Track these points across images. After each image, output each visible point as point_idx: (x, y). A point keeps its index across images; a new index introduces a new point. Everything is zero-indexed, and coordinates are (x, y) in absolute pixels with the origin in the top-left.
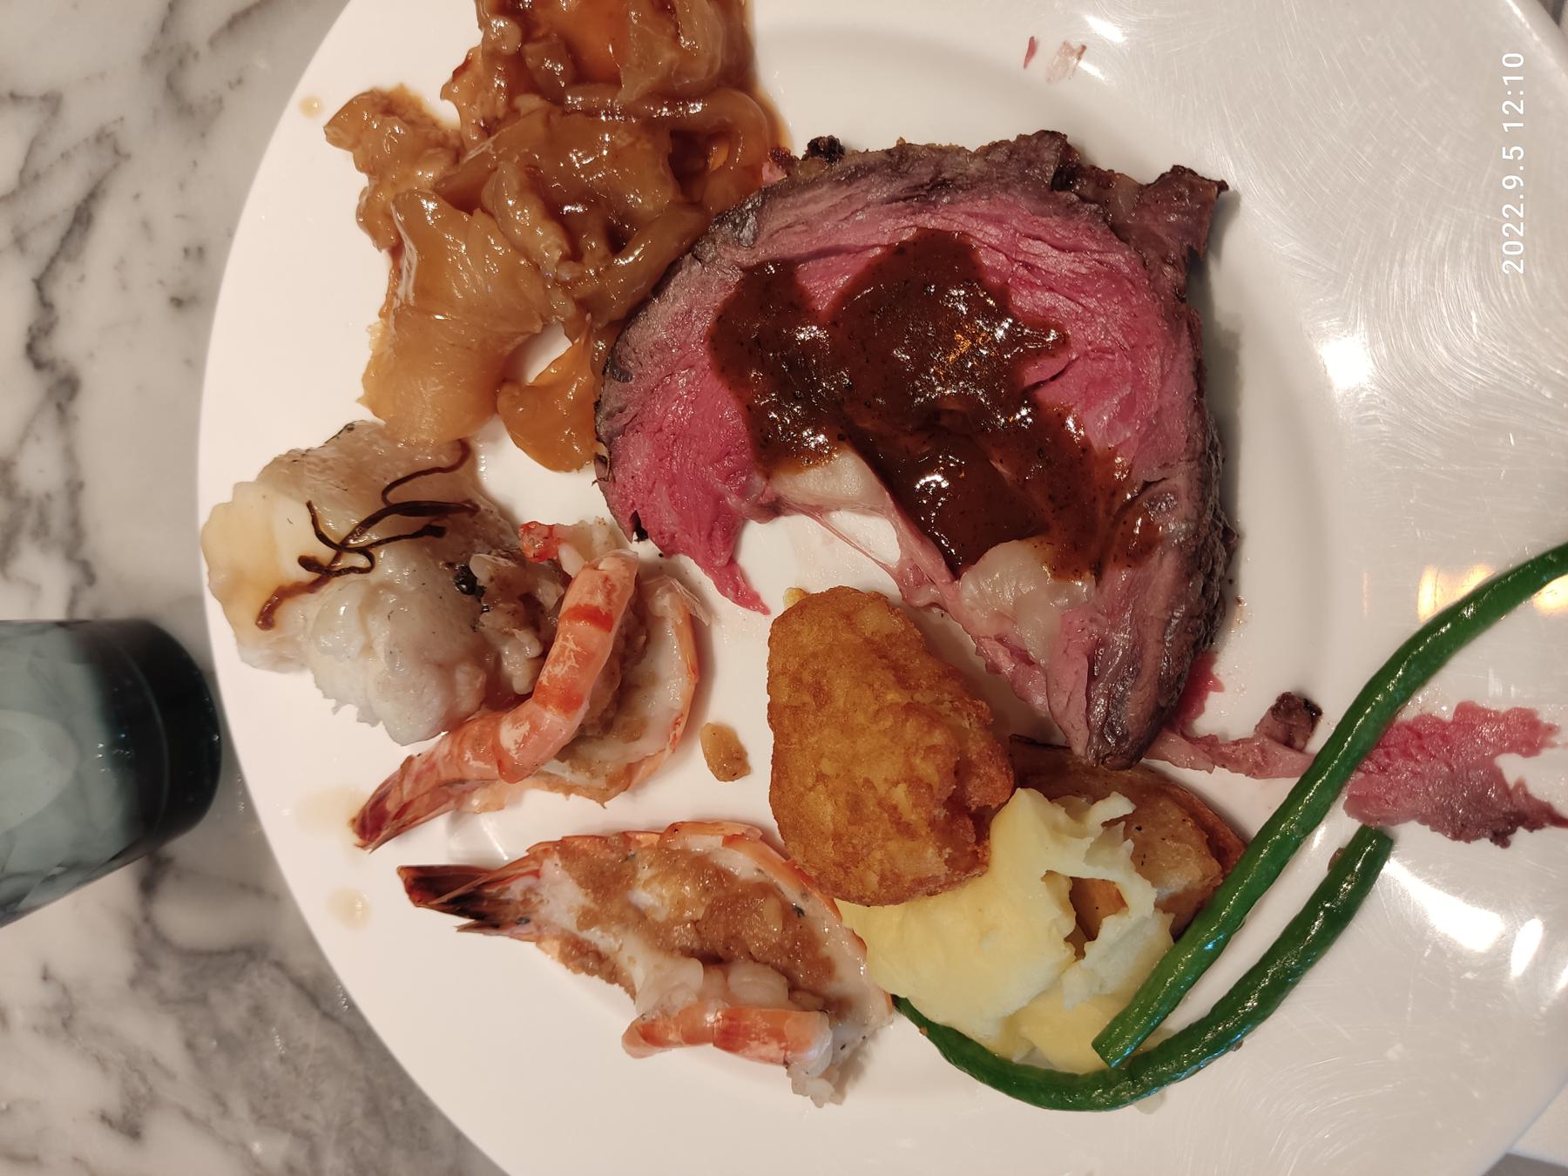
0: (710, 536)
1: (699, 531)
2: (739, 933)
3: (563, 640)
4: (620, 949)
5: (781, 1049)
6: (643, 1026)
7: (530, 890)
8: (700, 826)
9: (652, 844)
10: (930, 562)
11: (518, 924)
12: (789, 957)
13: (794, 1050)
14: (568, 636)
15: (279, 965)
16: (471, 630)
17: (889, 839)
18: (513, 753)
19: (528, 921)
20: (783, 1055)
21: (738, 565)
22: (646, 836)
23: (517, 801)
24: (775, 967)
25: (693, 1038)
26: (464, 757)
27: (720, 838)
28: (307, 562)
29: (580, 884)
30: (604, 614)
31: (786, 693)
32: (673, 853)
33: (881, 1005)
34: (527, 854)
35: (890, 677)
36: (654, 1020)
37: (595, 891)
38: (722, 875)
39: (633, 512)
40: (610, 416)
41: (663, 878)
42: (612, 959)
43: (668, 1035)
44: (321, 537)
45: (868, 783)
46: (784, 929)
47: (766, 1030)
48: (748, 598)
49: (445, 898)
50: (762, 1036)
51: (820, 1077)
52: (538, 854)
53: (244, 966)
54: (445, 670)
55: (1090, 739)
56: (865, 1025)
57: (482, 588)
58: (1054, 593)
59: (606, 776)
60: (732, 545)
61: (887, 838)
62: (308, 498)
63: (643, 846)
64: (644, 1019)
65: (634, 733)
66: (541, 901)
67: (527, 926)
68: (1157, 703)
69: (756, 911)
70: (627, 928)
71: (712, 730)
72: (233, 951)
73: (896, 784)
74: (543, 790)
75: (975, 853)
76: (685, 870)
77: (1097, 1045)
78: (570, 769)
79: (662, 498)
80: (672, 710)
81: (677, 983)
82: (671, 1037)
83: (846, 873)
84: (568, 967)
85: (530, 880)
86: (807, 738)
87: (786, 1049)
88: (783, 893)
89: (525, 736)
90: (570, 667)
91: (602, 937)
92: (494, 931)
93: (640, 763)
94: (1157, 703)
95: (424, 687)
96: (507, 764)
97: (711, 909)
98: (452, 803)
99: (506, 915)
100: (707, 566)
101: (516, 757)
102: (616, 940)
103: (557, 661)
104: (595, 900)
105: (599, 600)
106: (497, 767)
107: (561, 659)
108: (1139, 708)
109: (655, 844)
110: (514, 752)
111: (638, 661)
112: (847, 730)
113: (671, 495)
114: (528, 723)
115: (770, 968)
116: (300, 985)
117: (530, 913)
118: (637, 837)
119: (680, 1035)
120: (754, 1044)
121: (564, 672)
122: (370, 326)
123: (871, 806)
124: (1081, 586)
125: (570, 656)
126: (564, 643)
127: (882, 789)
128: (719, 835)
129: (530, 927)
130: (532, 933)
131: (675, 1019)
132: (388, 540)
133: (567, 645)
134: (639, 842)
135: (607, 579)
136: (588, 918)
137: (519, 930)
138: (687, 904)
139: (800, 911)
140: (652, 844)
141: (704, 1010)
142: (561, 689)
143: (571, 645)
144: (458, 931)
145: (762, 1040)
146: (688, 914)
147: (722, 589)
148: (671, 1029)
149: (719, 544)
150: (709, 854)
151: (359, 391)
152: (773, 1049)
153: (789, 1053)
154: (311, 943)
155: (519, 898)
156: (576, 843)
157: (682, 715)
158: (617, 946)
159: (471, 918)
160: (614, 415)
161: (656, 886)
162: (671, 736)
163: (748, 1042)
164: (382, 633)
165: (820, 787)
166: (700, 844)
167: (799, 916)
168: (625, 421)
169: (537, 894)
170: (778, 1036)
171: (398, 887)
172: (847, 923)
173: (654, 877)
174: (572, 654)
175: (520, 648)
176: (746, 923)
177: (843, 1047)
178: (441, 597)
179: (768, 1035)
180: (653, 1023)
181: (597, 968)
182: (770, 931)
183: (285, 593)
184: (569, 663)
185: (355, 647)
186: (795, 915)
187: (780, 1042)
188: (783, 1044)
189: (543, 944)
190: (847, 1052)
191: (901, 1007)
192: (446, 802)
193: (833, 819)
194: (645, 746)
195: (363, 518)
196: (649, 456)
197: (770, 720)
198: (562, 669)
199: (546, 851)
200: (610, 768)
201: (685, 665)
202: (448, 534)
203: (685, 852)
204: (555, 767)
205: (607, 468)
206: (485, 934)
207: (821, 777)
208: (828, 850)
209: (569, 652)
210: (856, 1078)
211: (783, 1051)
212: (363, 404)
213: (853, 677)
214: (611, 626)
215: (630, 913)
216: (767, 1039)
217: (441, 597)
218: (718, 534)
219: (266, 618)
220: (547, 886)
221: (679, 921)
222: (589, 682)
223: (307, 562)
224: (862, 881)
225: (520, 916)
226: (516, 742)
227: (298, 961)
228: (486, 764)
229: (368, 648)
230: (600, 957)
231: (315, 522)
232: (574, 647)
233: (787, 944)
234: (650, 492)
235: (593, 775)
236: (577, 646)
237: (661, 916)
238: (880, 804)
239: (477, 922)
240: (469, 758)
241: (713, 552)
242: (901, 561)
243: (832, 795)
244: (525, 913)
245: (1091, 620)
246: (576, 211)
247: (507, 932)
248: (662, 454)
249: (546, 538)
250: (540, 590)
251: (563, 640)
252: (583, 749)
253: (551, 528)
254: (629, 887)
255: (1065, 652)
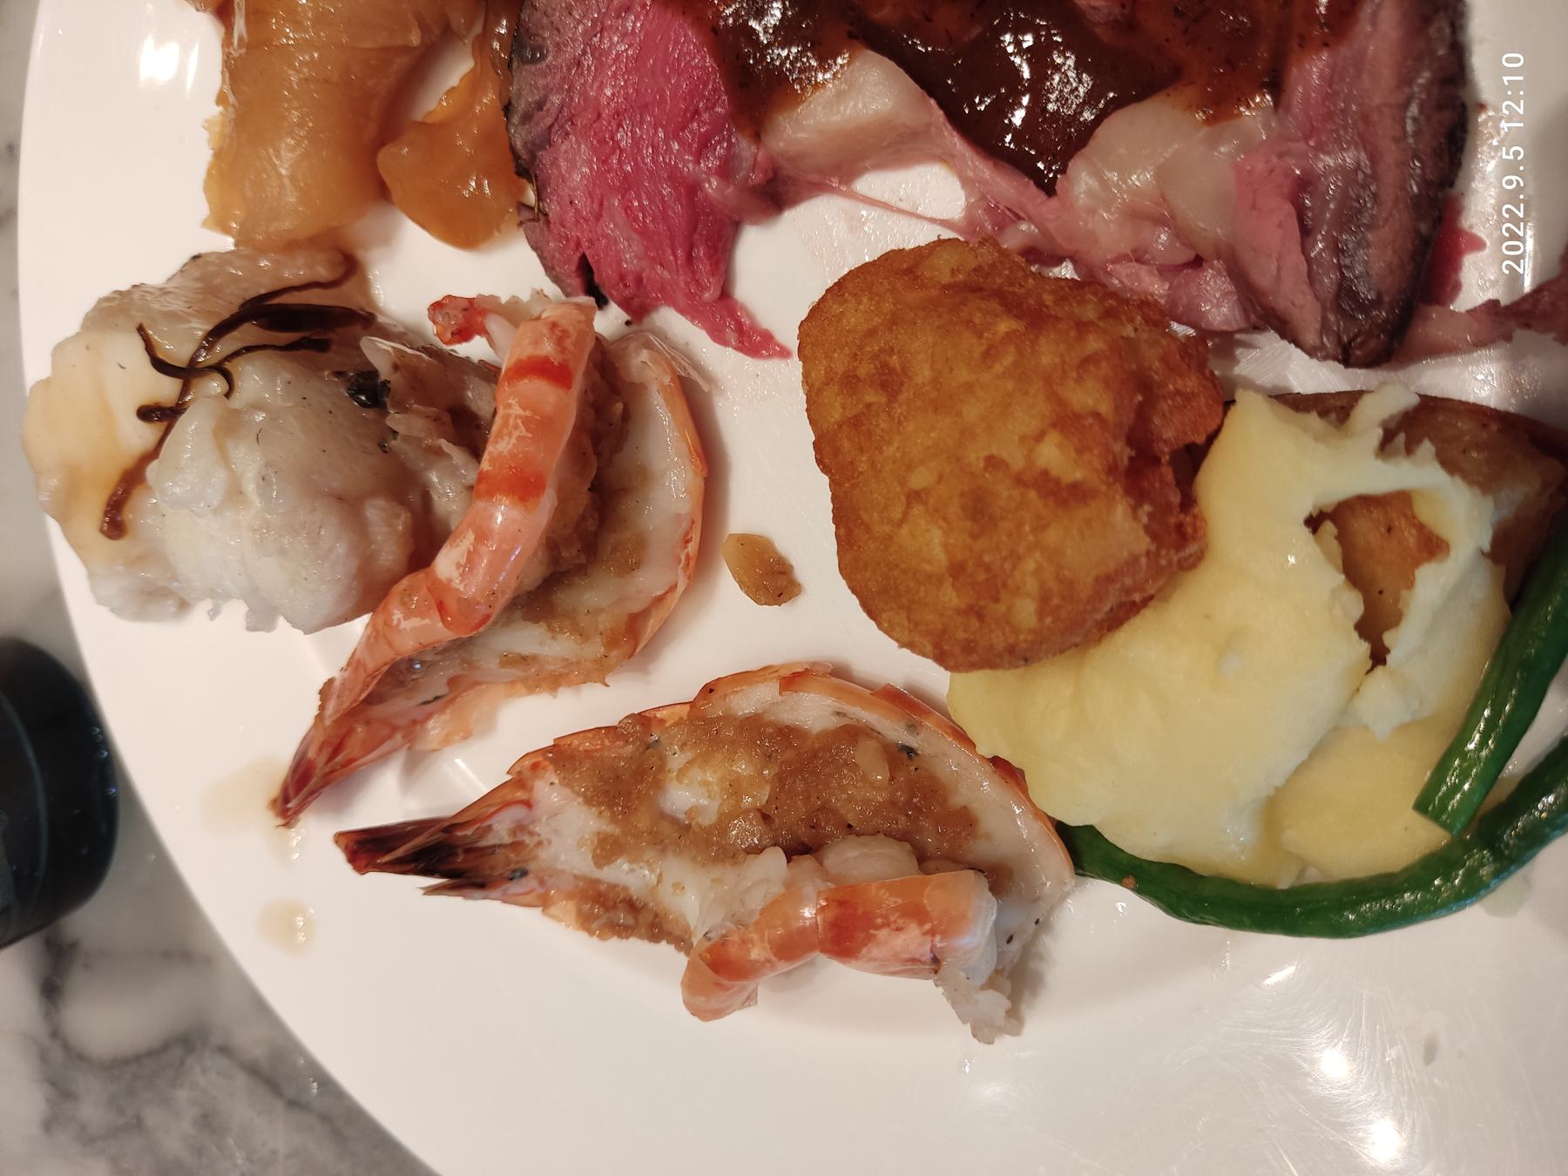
0: (689, 259)
1: (674, 254)
2: (828, 801)
3: (505, 408)
4: (659, 882)
5: (925, 934)
6: (710, 950)
7: (520, 828)
8: (743, 679)
9: (681, 718)
10: (1007, 186)
11: (511, 879)
12: (907, 815)
13: (945, 934)
14: (510, 401)
15: (224, 1050)
16: (380, 451)
17: (1045, 527)
18: (457, 584)
19: (524, 873)
20: (928, 948)
21: (733, 299)
22: (670, 710)
23: (489, 725)
24: (889, 834)
25: (792, 948)
26: (392, 620)
27: (775, 686)
28: (146, 413)
29: (589, 801)
30: (556, 363)
31: (837, 404)
32: (712, 722)
33: (1053, 860)
34: (509, 778)
35: (995, 305)
36: (724, 936)
37: (610, 806)
38: (787, 734)
39: (579, 255)
40: (527, 118)
41: (703, 759)
42: (651, 904)
43: (749, 950)
44: (161, 365)
45: (993, 462)
46: (892, 779)
47: (896, 909)
48: (755, 342)
49: (399, 852)
50: (892, 918)
51: (983, 988)
52: (527, 773)
53: (182, 1063)
54: (348, 505)
55: (1324, 320)
56: (1036, 900)
57: (386, 383)
58: (1213, 143)
59: (601, 634)
60: (722, 267)
61: (1040, 527)
62: (139, 320)
63: (667, 725)
64: (709, 939)
65: (630, 564)
66: (540, 844)
67: (524, 880)
68: (1417, 232)
69: (846, 764)
70: (663, 851)
71: (738, 540)
72: (166, 1046)
73: (1040, 437)
74: (522, 696)
75: (1180, 527)
76: (733, 742)
77: (1422, 806)
78: (550, 634)
79: (614, 227)
80: (679, 517)
81: (749, 884)
82: (757, 953)
83: (981, 617)
84: (591, 933)
85: (517, 813)
86: (881, 451)
87: (932, 932)
88: (879, 733)
89: (469, 552)
90: (520, 438)
91: (632, 870)
92: (478, 893)
93: (644, 614)
94: (1417, 232)
95: (320, 527)
96: (451, 604)
97: (780, 779)
98: (399, 737)
99: (493, 868)
100: (692, 311)
101: (461, 588)
102: (652, 871)
103: (500, 435)
104: (613, 820)
105: (547, 348)
106: (437, 616)
107: (505, 431)
108: (1390, 252)
109: (685, 717)
110: (458, 581)
111: (617, 447)
112: (942, 401)
113: (627, 208)
114: (471, 532)
115: (883, 837)
116: (253, 1070)
117: (526, 861)
118: (659, 715)
119: (767, 945)
120: (883, 934)
121: (510, 446)
122: (207, 121)
123: (1004, 492)
124: (1255, 113)
125: (517, 424)
126: (507, 411)
127: (1017, 462)
128: (772, 679)
129: (529, 883)
130: (532, 891)
131: (757, 923)
132: (249, 349)
133: (511, 411)
134: (662, 721)
135: (554, 325)
136: (607, 849)
137: (515, 888)
138: (745, 784)
139: (910, 751)
140: (681, 718)
141: (801, 901)
142: (510, 468)
143: (517, 410)
144: (425, 894)
145: (893, 926)
146: (747, 800)
147: (718, 336)
148: (752, 941)
149: (703, 267)
150: (764, 712)
151: (202, 209)
152: (912, 940)
153: (938, 938)
154: (261, 1008)
155: (507, 840)
156: (576, 742)
157: (693, 522)
158: (654, 878)
159: (442, 876)
160: (532, 116)
161: (697, 774)
162: (683, 557)
163: (873, 932)
164: (248, 461)
165: (917, 509)
166: (747, 703)
167: (910, 757)
168: (549, 121)
169: (531, 834)
170: (917, 913)
171: (339, 857)
172: (985, 750)
173: (690, 763)
174: (519, 421)
175: (453, 472)
176: (834, 784)
177: (1010, 940)
178: (330, 412)
179: (901, 916)
180: (723, 942)
181: (630, 921)
182: (873, 786)
183: (132, 479)
184: (516, 434)
185: (215, 494)
186: (904, 755)
187: (921, 923)
188: (927, 926)
189: (553, 910)
190: (1015, 946)
191: (1085, 865)
192: (389, 737)
193: (945, 546)
194: (649, 581)
195: (209, 327)
196: (589, 163)
197: (819, 461)
198: (508, 443)
199: (535, 767)
200: (604, 622)
201: (685, 447)
202: (334, 347)
203: (728, 718)
204: (528, 638)
205: (536, 222)
206: (465, 897)
207: (915, 497)
208: (951, 597)
209: (515, 419)
210: (1034, 993)
211: (929, 938)
212: (211, 228)
213: (939, 327)
214: (571, 382)
215: (665, 827)
216: (900, 922)
217: (330, 412)
218: (700, 251)
219: (115, 523)
220: (545, 818)
221: (738, 812)
222: (551, 458)
223: (146, 413)
224: (1008, 623)
225: (513, 866)
226: (458, 565)
227: (249, 1039)
228: (423, 618)
229: (235, 494)
230: (633, 906)
231: (149, 347)
232: (520, 412)
233: (901, 797)
234: (598, 217)
235: (583, 635)
236: (524, 409)
237: (709, 818)
238: (1019, 480)
239: (452, 881)
240: (399, 619)
241: (697, 282)
242: (969, 208)
243: (937, 513)
244: (518, 863)
245: (1281, 156)
246: (488, 184)
247: (497, 893)
248: (605, 148)
249: (466, 310)
250: (470, 394)
251: (505, 408)
252: (563, 598)
253: (471, 301)
254: (658, 785)
255: (1254, 207)
